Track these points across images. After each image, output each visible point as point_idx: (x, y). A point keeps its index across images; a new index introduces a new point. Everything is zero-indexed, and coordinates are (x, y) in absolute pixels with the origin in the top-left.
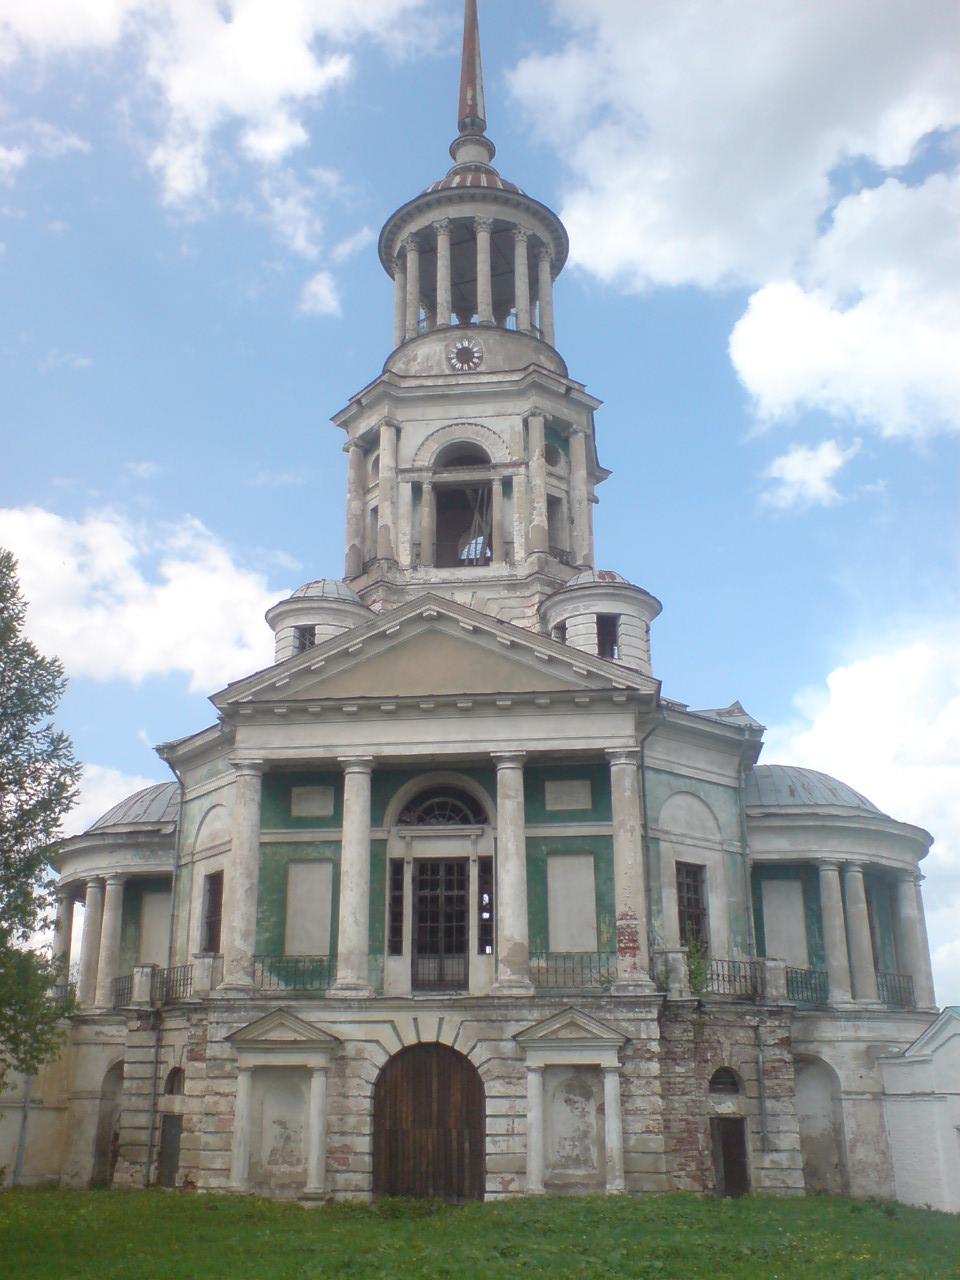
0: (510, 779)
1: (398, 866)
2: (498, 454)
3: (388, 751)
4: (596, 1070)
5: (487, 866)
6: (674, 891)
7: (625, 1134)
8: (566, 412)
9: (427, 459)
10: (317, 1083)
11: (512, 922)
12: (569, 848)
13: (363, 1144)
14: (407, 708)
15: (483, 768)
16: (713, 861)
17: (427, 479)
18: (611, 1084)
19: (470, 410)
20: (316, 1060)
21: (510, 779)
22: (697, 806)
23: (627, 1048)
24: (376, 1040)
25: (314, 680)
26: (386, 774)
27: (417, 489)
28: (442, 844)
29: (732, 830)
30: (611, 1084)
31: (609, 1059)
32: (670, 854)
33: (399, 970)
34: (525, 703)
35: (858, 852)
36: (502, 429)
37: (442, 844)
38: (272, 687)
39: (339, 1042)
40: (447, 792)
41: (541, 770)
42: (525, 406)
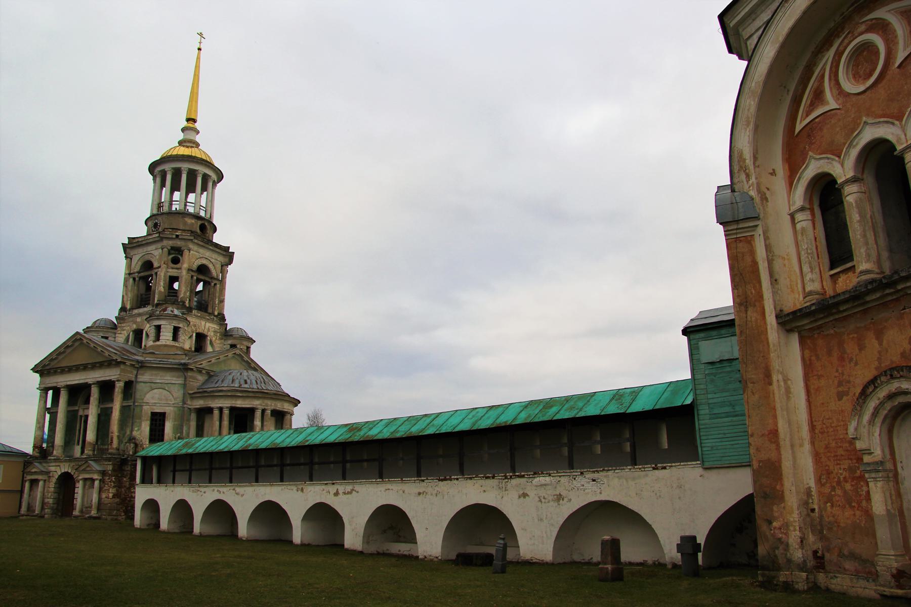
1: (81, 416)
2: (156, 265)
3: (69, 383)
4: (93, 480)
6: (149, 422)
7: (100, 499)
9: (137, 269)
10: (41, 483)
13: (51, 501)
14: (71, 370)
16: (169, 410)
18: (97, 483)
20: (40, 477)
22: (165, 392)
23: (104, 473)
24: (58, 470)
25: (56, 362)
27: (134, 279)
29: (179, 400)
30: (97, 483)
31: (95, 476)
32: (147, 410)
34: (94, 366)
35: (226, 403)
38: (45, 366)
39: (49, 472)
42: (159, 245)
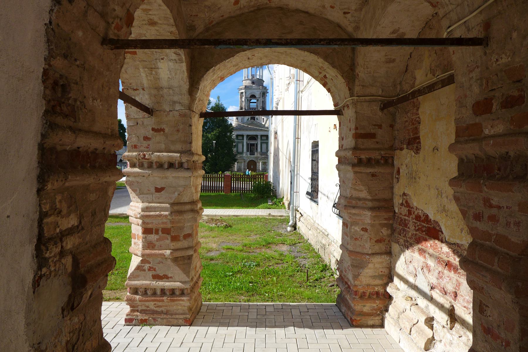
0: (259, 137)
2: (257, 96)
5: (257, 144)
8: (265, 91)
9: (249, 96)
11: (259, 150)
12: (264, 143)
15: (257, 136)
17: (249, 99)
19: (254, 91)
21: (259, 137)
26: (248, 136)
28: (253, 142)
33: (249, 153)
36: (257, 93)
37: (253, 142)
40: (253, 138)
41: (262, 136)
